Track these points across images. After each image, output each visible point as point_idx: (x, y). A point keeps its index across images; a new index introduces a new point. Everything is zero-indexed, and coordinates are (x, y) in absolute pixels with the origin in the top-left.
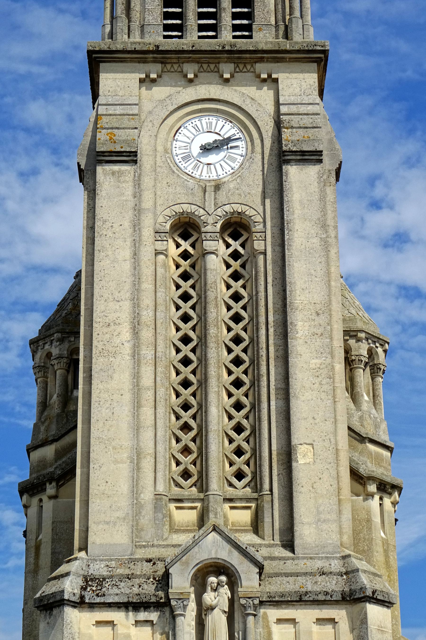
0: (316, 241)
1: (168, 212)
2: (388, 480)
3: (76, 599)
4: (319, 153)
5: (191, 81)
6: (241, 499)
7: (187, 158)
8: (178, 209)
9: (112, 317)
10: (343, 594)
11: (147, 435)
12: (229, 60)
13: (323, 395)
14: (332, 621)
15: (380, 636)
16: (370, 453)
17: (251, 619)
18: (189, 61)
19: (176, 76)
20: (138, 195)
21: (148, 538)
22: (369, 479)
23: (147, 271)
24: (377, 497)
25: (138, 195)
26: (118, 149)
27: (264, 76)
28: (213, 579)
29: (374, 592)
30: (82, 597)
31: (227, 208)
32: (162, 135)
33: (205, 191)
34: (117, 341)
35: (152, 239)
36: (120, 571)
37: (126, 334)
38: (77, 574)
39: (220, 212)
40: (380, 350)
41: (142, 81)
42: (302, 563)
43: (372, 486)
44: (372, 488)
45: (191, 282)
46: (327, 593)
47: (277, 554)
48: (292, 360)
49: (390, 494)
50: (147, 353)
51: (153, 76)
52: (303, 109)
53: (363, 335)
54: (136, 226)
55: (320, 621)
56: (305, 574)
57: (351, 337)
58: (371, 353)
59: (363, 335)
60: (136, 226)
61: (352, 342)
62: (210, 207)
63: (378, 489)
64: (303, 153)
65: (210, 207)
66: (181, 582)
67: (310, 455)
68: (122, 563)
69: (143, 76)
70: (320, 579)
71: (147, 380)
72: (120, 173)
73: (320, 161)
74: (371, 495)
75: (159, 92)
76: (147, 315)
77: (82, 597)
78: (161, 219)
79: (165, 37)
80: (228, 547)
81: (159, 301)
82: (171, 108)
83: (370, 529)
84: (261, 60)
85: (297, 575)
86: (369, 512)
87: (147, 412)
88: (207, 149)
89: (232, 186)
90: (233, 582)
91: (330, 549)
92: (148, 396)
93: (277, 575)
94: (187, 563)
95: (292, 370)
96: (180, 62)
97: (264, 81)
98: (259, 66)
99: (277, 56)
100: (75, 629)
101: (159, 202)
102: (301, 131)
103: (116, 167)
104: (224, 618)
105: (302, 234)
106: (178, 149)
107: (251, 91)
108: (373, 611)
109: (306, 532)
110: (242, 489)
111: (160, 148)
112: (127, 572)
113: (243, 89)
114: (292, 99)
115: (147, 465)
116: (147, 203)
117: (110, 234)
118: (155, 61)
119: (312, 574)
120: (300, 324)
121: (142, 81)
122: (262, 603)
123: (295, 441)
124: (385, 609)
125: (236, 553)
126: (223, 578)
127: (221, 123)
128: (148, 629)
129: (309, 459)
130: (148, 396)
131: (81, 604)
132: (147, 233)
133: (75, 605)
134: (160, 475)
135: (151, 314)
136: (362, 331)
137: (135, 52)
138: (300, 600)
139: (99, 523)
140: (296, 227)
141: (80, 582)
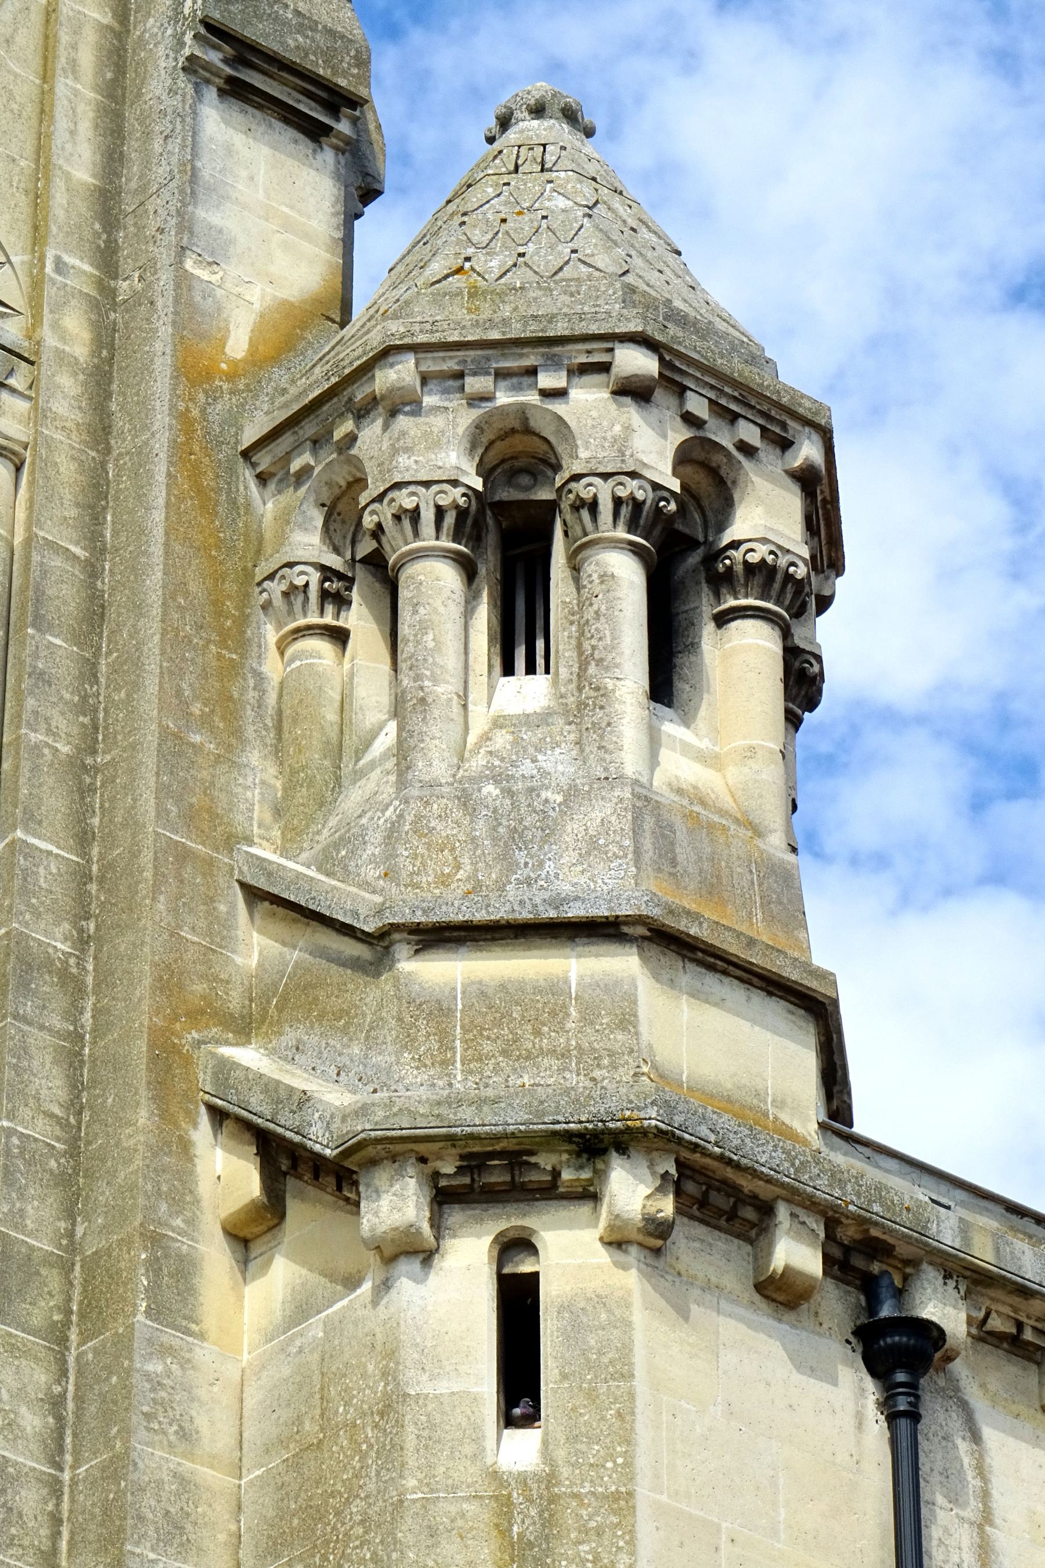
2: (514, 1118)
16: (437, 1010)
22: (373, 1163)
43: (385, 1202)
44: (396, 1203)
49: (589, 1195)
59: (402, 373)
61: (372, 439)
63: (443, 1198)
74: (411, 1252)
83: (390, 1453)
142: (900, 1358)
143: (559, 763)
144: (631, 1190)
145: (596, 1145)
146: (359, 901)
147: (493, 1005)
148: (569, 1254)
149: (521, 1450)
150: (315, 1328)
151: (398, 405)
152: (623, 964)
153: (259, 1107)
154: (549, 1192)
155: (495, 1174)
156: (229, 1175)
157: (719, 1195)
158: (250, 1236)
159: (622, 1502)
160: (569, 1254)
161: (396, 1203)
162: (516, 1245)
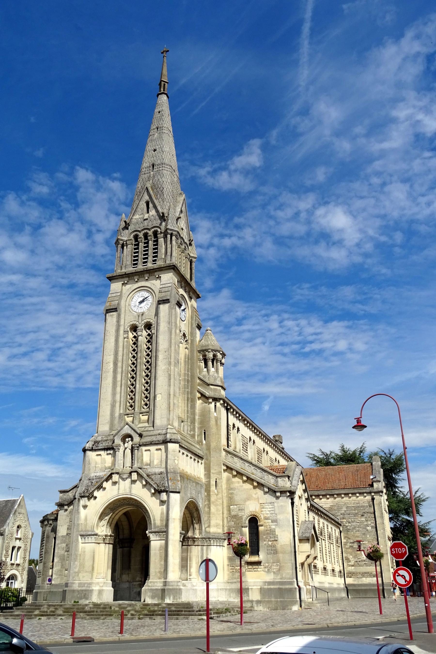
0: (166, 328)
1: (128, 325)
3: (90, 448)
4: (168, 300)
5: (137, 281)
6: (145, 413)
7: (135, 306)
8: (131, 323)
9: (108, 361)
10: (163, 441)
11: (118, 396)
12: (147, 273)
13: (165, 378)
14: (160, 449)
15: (173, 453)
16: (212, 389)
17: (136, 451)
18: (136, 275)
19: (133, 280)
20: (118, 321)
21: (116, 427)
23: (121, 344)
24: (213, 403)
25: (118, 321)
26: (112, 308)
27: (157, 276)
28: (127, 439)
29: (170, 440)
30: (92, 448)
31: (145, 321)
32: (128, 300)
33: (139, 316)
34: (109, 368)
35: (123, 334)
36: (104, 439)
37: (111, 365)
38: (92, 441)
39: (143, 322)
40: (218, 354)
41: (123, 284)
42: (155, 431)
44: (211, 400)
45: (136, 345)
46: (158, 441)
47: (149, 429)
48: (157, 367)
49: (219, 401)
50: (119, 370)
51: (126, 282)
52: (167, 285)
53: (210, 350)
54: (118, 331)
55: (157, 450)
56: (154, 435)
57: (207, 351)
58: (215, 356)
59: (210, 350)
60: (118, 331)
61: (207, 353)
62: (140, 321)
63: (213, 400)
64: (164, 300)
65: (140, 321)
66: (118, 441)
67: (160, 397)
68: (106, 436)
69: (123, 282)
70: (158, 436)
71: (119, 378)
73: (169, 302)
75: (128, 286)
76: (120, 358)
77: (92, 448)
78: (126, 327)
79: (133, 268)
80: (130, 429)
81: (124, 353)
82: (131, 291)
83: (210, 414)
84: (156, 271)
85: (152, 436)
86: (209, 408)
87: (118, 389)
88: (141, 302)
89: (147, 313)
90: (132, 440)
91: (164, 426)
92: (119, 384)
93: (147, 436)
94: (119, 435)
95: (157, 371)
96: (133, 276)
97: (157, 277)
98: (156, 273)
99: (161, 269)
100: (90, 457)
101: (126, 322)
102: (164, 293)
103: (112, 314)
104: (130, 451)
105: (163, 327)
106: (133, 304)
107: (154, 282)
108: (170, 445)
109: (158, 422)
110: (146, 409)
111: (127, 305)
112: (106, 439)
113: (152, 282)
114: (165, 283)
115: (117, 405)
116: (122, 322)
117: (109, 335)
118: (126, 277)
119: (156, 435)
120: (160, 356)
121: (123, 284)
122: (140, 446)
123: (156, 393)
124: (176, 444)
125: (133, 431)
126: (130, 439)
127: (145, 293)
128: (110, 456)
129: (160, 399)
130: (119, 384)
131: (92, 450)
132: (121, 332)
133: (90, 450)
134: (121, 407)
135: (121, 358)
136: (209, 349)
137: (119, 275)
138: (151, 444)
139: (101, 425)
140: (161, 324)
141: (93, 443)
142: (227, 410)
143: (216, 374)
144: (222, 402)
145: (220, 399)
146: (208, 382)
147: (214, 389)
148: (218, 404)
149: (215, 414)
150: (204, 405)
151: (209, 352)
152: (220, 388)
153: (202, 392)
155: (215, 400)
156: (199, 395)
157: (224, 402)
158: (199, 398)
159: (221, 418)
161: (211, 400)
162: (215, 403)
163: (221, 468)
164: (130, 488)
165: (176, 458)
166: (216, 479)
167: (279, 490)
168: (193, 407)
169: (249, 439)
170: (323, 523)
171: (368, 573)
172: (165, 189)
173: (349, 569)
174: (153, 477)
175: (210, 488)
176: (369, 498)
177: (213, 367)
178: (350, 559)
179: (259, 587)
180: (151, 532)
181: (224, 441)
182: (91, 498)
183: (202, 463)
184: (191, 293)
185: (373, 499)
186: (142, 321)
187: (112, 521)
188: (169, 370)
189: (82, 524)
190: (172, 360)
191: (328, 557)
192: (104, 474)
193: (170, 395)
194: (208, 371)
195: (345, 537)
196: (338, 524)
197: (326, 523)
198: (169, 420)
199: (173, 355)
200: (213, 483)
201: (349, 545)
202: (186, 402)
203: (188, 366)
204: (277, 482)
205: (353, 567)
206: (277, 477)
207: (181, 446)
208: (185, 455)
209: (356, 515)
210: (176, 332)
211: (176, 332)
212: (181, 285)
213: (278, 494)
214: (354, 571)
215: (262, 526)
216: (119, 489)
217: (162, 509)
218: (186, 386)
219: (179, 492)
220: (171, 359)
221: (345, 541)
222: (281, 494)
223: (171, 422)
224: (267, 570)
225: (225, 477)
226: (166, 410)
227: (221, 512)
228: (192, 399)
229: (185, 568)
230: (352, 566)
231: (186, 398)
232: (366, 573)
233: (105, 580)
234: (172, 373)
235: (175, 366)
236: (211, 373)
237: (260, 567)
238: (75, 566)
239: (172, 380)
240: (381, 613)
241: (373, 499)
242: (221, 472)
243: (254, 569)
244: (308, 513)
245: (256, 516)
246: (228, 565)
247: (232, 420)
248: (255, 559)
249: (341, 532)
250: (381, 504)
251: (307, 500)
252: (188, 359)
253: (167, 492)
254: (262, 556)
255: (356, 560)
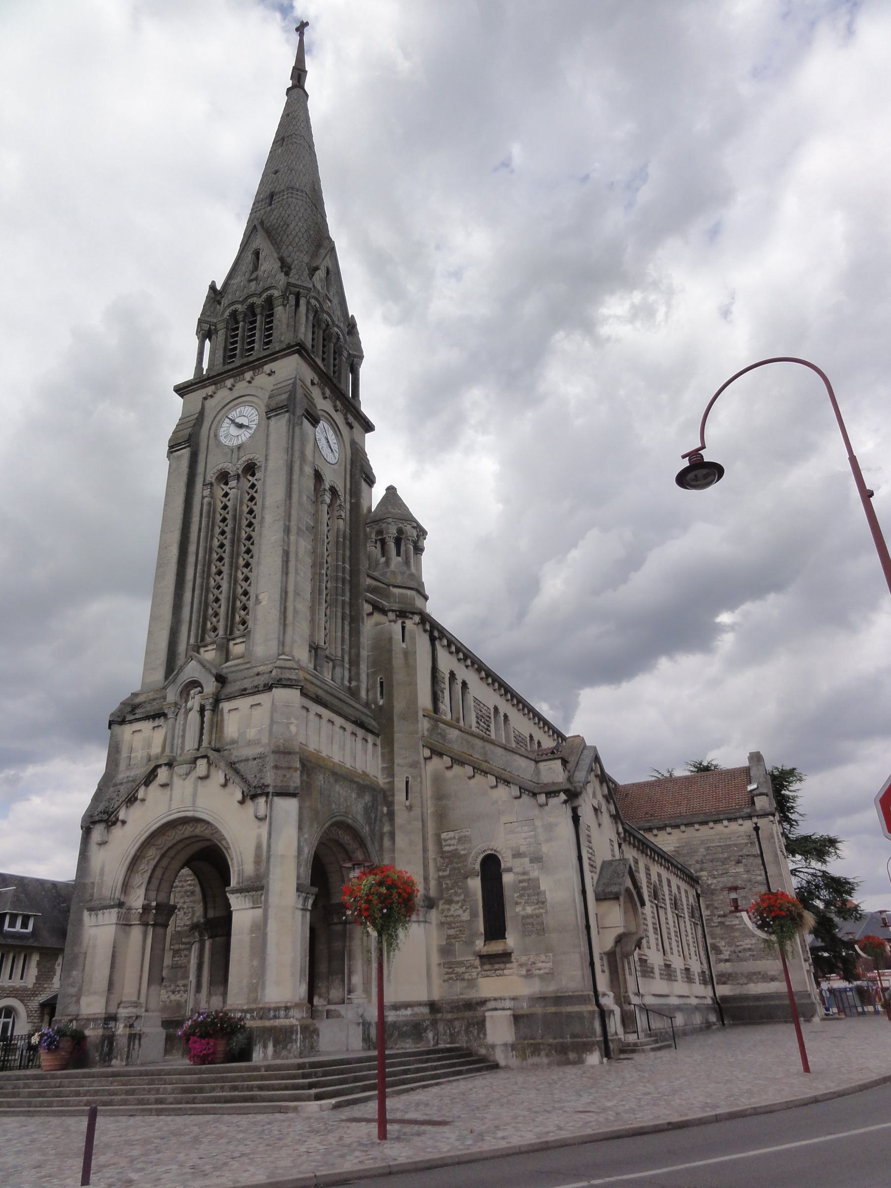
8: (220, 467)
24: (400, 622)
50: (191, 559)
59: (390, 520)
63: (397, 616)
72: (182, 455)
87: (188, 596)
99: (274, 357)
116: (200, 468)
124: (295, 690)
130: (189, 586)
144: (417, 618)
148: (409, 624)
149: (404, 645)
154: (407, 617)
156: (368, 608)
160: (409, 624)
161: (392, 616)
163: (419, 754)
164: (195, 795)
165: (293, 720)
166: (407, 777)
167: (543, 790)
168: (355, 632)
169: (492, 710)
170: (659, 875)
171: (759, 973)
172: (292, 227)
173: (721, 967)
174: (240, 766)
175: (393, 795)
176: (748, 825)
177: (398, 554)
178: (722, 948)
179: (509, 1012)
180: (234, 892)
181: (424, 700)
182: (114, 823)
183: (375, 745)
184: (349, 416)
185: (757, 829)
186: (239, 459)
187: (163, 874)
188: (286, 543)
189: (93, 883)
190: (293, 524)
191: (674, 944)
192: (141, 771)
193: (286, 593)
194: (387, 563)
195: (707, 907)
196: (693, 881)
197: (665, 874)
198: (282, 643)
199: (294, 512)
200: (400, 785)
201: (716, 920)
202: (339, 621)
203: (344, 551)
204: (537, 772)
205: (728, 964)
206: (537, 762)
207: (304, 694)
208: (324, 722)
209: (724, 862)
210: (301, 470)
211: (301, 470)
212: (323, 394)
213: (542, 798)
214: (730, 971)
215: (510, 870)
216: (171, 800)
217: (259, 837)
218: (340, 591)
219: (294, 795)
220: (289, 521)
221: (708, 913)
222: (547, 798)
223: (287, 649)
224: (524, 972)
225: (429, 774)
226: (277, 624)
227: (420, 847)
228: (351, 616)
229: (340, 976)
230: (726, 961)
231: (339, 615)
232: (754, 974)
233: (143, 1010)
234: (292, 549)
235: (298, 534)
236: (393, 566)
237: (508, 965)
238: (71, 980)
239: (292, 564)
240: (807, 1069)
241: (757, 829)
242: (418, 762)
243: (496, 970)
244: (620, 846)
245: (495, 851)
246: (439, 964)
247: (447, 662)
248: (496, 947)
249: (698, 896)
250: (773, 838)
251: (616, 817)
252: (344, 538)
253: (267, 795)
254: (511, 940)
255: (732, 949)
